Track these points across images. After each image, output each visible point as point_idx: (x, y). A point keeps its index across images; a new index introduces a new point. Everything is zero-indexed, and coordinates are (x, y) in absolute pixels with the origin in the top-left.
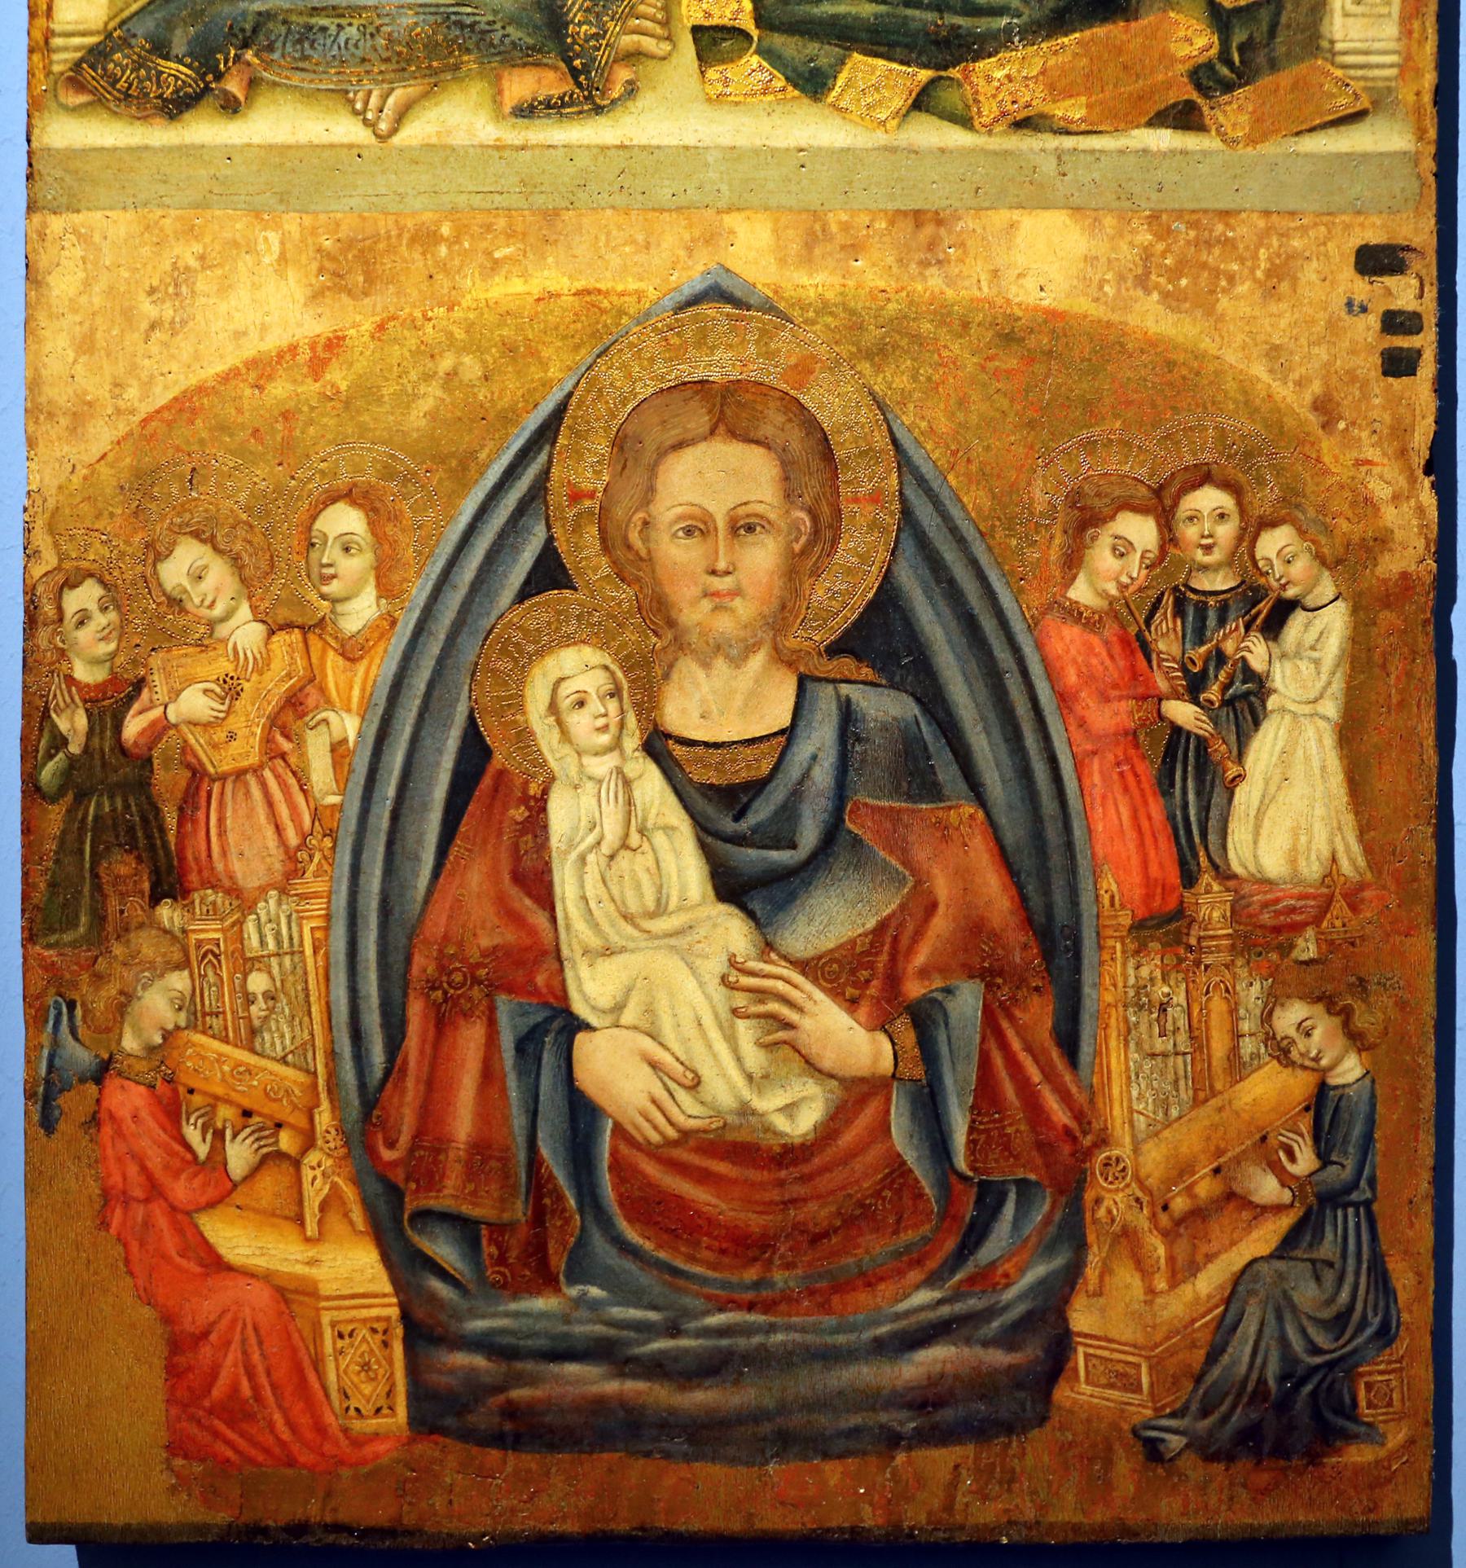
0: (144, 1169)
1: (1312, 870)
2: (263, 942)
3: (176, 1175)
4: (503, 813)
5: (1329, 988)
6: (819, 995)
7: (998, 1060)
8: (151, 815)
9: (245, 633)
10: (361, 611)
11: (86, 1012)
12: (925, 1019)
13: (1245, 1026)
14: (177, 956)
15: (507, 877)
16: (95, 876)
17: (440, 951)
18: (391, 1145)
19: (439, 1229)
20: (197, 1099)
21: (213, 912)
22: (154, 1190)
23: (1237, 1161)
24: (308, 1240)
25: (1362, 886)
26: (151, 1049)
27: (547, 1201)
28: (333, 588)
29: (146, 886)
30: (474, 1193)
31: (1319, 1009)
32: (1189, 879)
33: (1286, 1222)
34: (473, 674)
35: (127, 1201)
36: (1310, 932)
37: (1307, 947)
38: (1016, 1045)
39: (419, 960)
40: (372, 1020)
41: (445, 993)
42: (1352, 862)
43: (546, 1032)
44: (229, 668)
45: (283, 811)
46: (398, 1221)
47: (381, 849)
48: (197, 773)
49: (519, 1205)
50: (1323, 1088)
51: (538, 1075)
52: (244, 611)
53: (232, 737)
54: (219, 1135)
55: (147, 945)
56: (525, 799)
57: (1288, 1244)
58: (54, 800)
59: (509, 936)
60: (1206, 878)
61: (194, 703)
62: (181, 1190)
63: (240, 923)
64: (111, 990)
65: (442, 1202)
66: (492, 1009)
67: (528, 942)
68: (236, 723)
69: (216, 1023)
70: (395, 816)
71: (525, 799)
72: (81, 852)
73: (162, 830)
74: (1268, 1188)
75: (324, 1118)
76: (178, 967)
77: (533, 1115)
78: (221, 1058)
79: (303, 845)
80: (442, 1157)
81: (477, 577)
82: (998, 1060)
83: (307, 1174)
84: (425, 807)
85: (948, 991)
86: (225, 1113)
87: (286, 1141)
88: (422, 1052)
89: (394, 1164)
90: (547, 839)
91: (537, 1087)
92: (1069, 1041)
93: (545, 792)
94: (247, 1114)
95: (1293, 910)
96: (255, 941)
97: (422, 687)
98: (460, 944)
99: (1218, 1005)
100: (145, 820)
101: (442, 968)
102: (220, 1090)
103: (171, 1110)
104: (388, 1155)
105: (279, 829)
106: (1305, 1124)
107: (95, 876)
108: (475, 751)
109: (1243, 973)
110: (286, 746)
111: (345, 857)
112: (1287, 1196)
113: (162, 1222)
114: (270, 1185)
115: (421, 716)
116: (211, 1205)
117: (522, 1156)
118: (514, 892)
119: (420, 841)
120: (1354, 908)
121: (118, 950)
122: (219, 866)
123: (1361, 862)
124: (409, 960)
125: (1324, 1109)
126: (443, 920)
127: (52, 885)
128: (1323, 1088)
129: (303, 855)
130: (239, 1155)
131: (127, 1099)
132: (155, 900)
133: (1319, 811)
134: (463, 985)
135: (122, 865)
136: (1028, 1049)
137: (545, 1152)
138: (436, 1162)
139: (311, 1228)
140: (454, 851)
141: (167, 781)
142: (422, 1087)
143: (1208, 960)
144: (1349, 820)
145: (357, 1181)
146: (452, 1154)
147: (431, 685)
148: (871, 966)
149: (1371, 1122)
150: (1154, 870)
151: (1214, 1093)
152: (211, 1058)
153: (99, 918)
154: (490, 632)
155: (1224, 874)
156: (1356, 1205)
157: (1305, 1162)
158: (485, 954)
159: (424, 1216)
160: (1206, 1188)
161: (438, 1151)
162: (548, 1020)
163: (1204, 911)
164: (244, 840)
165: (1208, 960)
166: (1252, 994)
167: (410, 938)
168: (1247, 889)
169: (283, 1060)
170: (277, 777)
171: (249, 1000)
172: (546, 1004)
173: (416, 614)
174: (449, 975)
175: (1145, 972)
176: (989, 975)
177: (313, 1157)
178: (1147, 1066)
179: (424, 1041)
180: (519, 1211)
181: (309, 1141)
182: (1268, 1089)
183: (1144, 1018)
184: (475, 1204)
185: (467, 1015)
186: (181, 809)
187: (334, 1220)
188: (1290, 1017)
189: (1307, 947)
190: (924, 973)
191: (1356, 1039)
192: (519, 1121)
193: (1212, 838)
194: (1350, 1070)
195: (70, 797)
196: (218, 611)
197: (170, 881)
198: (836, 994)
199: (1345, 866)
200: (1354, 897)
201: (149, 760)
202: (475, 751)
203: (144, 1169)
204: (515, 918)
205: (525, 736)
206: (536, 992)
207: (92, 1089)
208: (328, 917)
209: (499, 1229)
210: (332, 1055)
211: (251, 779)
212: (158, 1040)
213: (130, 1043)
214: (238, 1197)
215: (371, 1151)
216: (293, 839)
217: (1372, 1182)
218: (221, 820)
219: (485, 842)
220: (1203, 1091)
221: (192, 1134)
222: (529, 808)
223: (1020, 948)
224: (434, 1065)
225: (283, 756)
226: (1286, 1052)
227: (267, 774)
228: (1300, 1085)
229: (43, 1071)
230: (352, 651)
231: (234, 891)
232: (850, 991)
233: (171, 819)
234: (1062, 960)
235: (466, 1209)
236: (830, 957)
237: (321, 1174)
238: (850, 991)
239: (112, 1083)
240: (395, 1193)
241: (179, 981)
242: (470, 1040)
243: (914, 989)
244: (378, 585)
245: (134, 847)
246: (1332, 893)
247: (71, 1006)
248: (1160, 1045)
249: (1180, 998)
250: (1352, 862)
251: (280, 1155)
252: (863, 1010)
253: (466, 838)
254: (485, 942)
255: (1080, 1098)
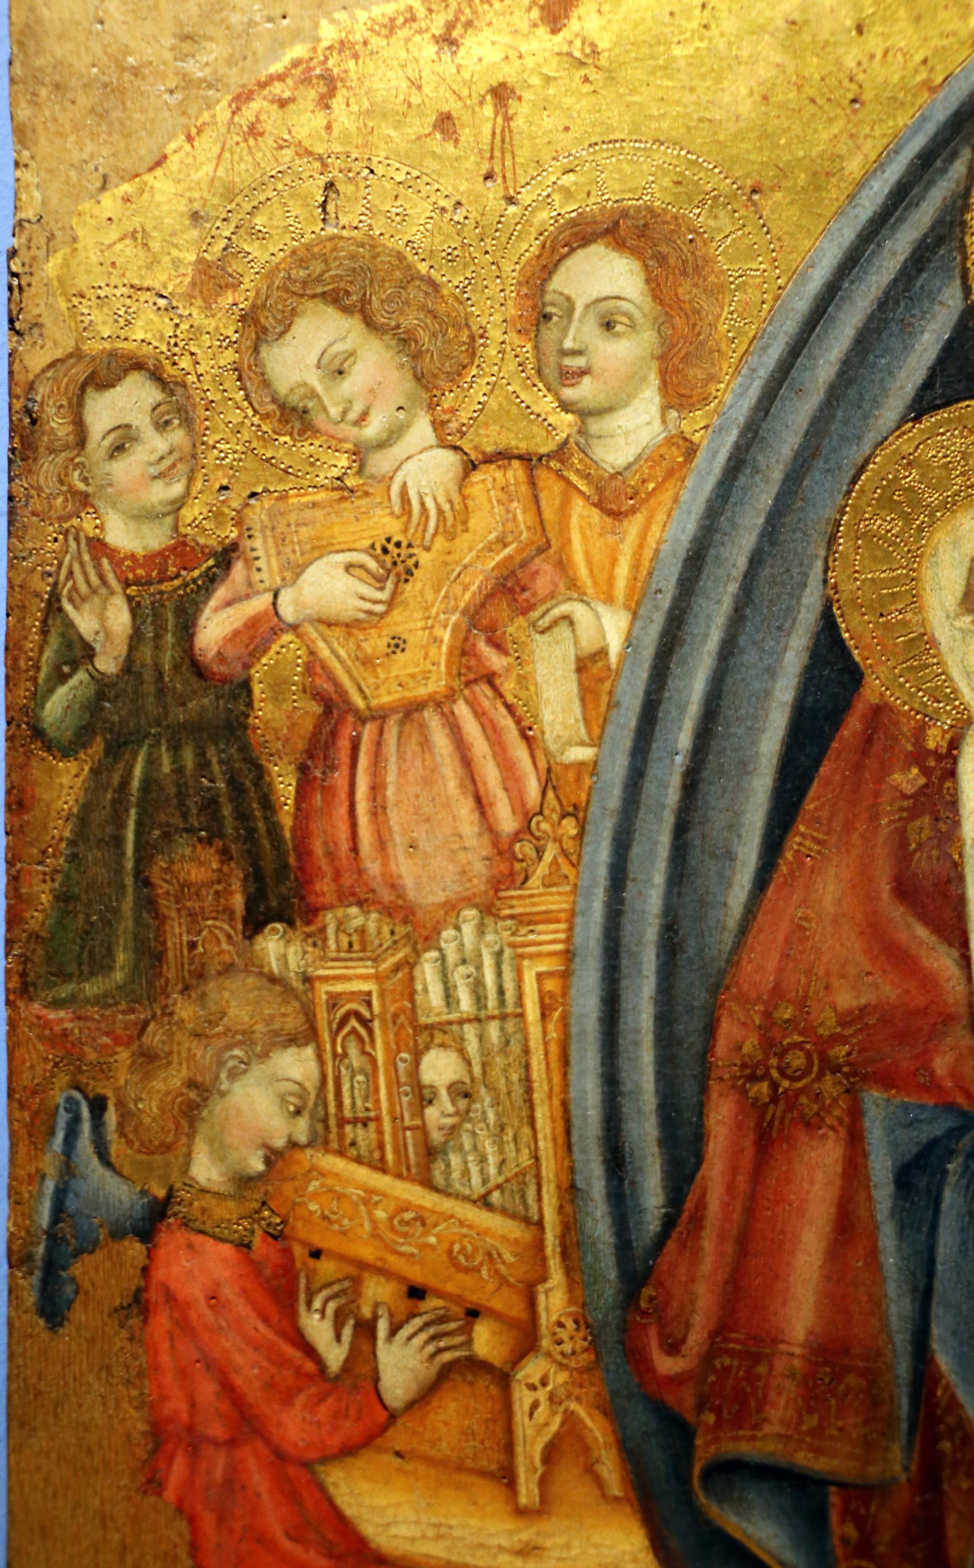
0: (228, 1388)
2: (449, 997)
3: (287, 1399)
4: (880, 780)
8: (249, 781)
9: (424, 468)
10: (634, 430)
11: (125, 1115)
14: (293, 1022)
15: (885, 888)
16: (143, 881)
17: (767, 1015)
18: (673, 1348)
19: (753, 1493)
20: (327, 1268)
21: (360, 946)
22: (246, 1423)
24: (521, 1512)
26: (244, 1182)
27: (946, 1446)
28: (583, 392)
29: (238, 901)
30: (818, 1432)
34: (832, 540)
35: (195, 1443)
39: (728, 1029)
40: (644, 1131)
41: (774, 1086)
43: (950, 1154)
44: (393, 527)
45: (491, 774)
46: (685, 1481)
47: (665, 839)
48: (333, 708)
49: (896, 1452)
51: (934, 1227)
52: (422, 431)
53: (397, 645)
54: (366, 1329)
55: (237, 1002)
56: (919, 756)
58: (67, 751)
59: (887, 990)
61: (329, 586)
62: (295, 1425)
63: (409, 965)
64: (171, 1080)
65: (764, 1444)
66: (856, 1113)
67: (920, 1000)
68: (405, 621)
69: (364, 1137)
70: (692, 783)
71: (919, 756)
72: (118, 841)
73: (268, 805)
75: (554, 1301)
76: (293, 1040)
77: (924, 1297)
78: (370, 1197)
79: (525, 830)
80: (762, 1369)
81: (841, 374)
83: (522, 1398)
84: (745, 768)
86: (377, 1291)
87: (486, 1341)
88: (730, 1188)
89: (676, 1381)
90: (957, 824)
91: (932, 1248)
93: (955, 744)
94: (416, 1293)
96: (435, 997)
97: (742, 562)
98: (802, 1004)
100: (234, 784)
101: (768, 1044)
102: (368, 1253)
103: (280, 1287)
104: (666, 1365)
105: (481, 804)
107: (143, 881)
108: (834, 669)
110: (495, 661)
111: (600, 853)
113: (259, 1480)
114: (453, 1416)
115: (738, 618)
116: (348, 1451)
117: (903, 1368)
118: (897, 914)
119: (734, 827)
121: (185, 1010)
122: (373, 867)
124: (710, 1030)
126: (772, 964)
127: (64, 898)
129: (525, 849)
130: (401, 1364)
131: (198, 1267)
132: (255, 923)
134: (807, 1072)
135: (195, 864)
137: (944, 1361)
138: (751, 1377)
139: (527, 1492)
140: (794, 842)
141: (276, 713)
142: (729, 1248)
145: (611, 1410)
146: (780, 1364)
147: (756, 560)
152: (354, 1196)
153: (151, 956)
154: (862, 469)
158: (845, 1019)
159: (728, 1472)
161: (757, 1358)
162: (955, 1134)
164: (419, 822)
167: (715, 990)
169: (484, 1202)
170: (480, 714)
171: (424, 1097)
172: (950, 1107)
173: (732, 437)
174: (781, 1056)
177: (532, 1369)
179: (734, 1170)
180: (896, 1462)
181: (527, 1339)
184: (818, 1451)
185: (810, 1126)
186: (303, 769)
187: (569, 1478)
192: (899, 1307)
195: (98, 747)
196: (373, 429)
197: (280, 891)
201: (246, 685)
202: (834, 669)
203: (228, 1388)
204: (896, 957)
205: (923, 644)
206: (933, 1086)
207: (135, 1249)
208: (569, 955)
209: (860, 1494)
210: (571, 1192)
211: (432, 718)
212: (257, 1165)
213: (205, 1170)
214: (398, 1437)
215: (637, 1359)
216: (507, 821)
218: (376, 789)
219: (848, 827)
221: (317, 1327)
222: (925, 771)
224: (750, 1212)
225: (490, 679)
227: (462, 709)
229: (44, 1215)
230: (615, 500)
231: (399, 910)
233: (285, 785)
235: (803, 1459)
237: (545, 1399)
239: (172, 1240)
240: (679, 1432)
241: (297, 1065)
242: (816, 1168)
244: (664, 387)
245: (215, 833)
247: (98, 1106)
251: (475, 1365)
253: (815, 821)
254: (846, 999)
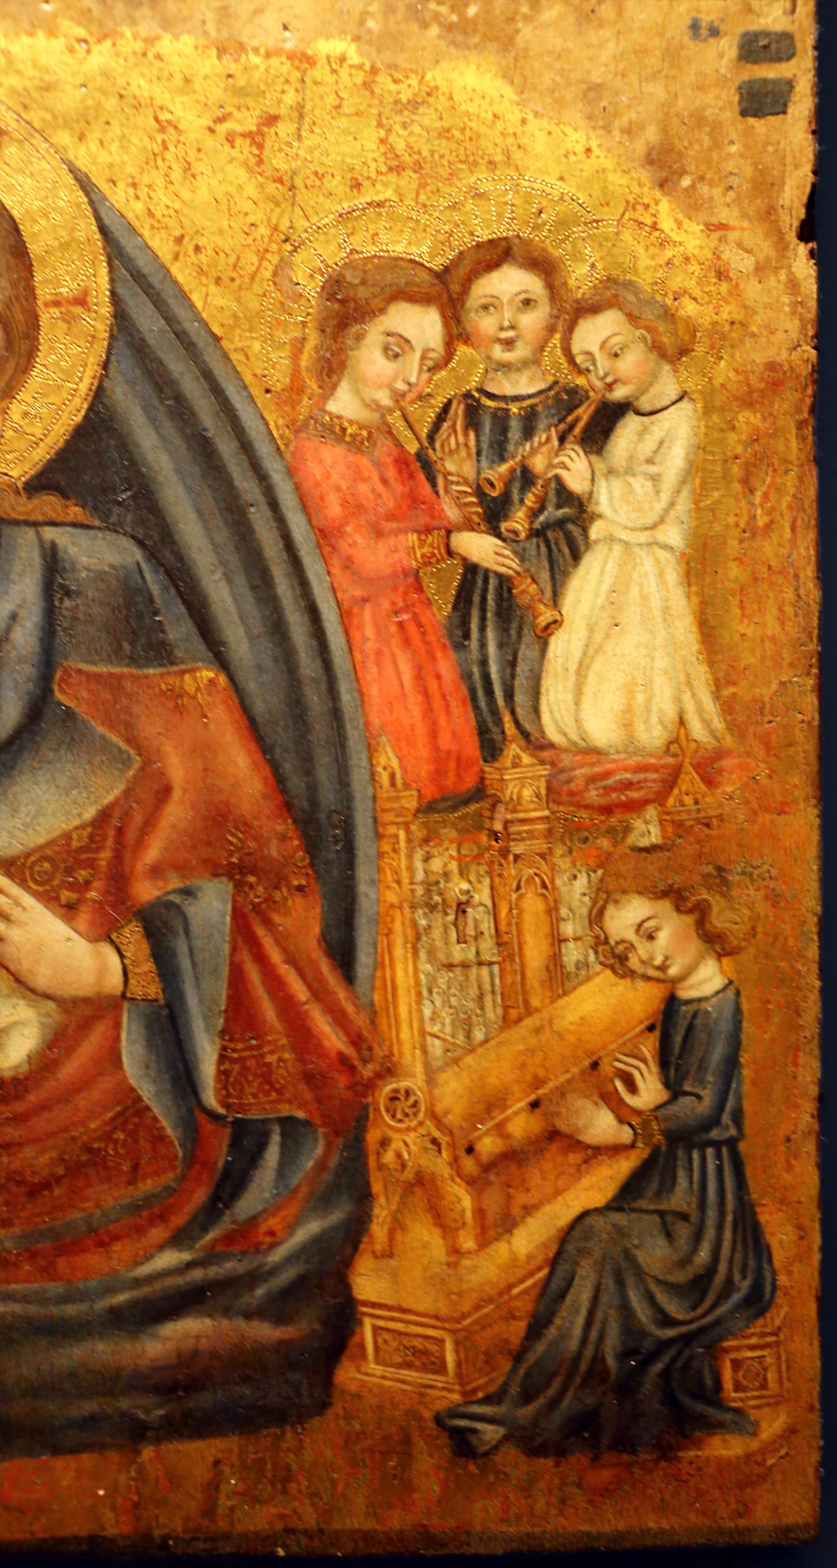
1: (652, 736)
5: (677, 880)
6: (28, 900)
7: (253, 974)
12: (160, 928)
13: (568, 929)
23: (561, 1092)
25: (719, 754)
31: (665, 906)
32: (491, 749)
33: (625, 1166)
36: (651, 812)
37: (647, 830)
38: (276, 956)
42: (705, 724)
50: (672, 1004)
57: (629, 1193)
60: (513, 749)
74: (601, 1125)
82: (253, 974)
85: (188, 892)
92: (342, 952)
95: (628, 785)
99: (533, 904)
106: (649, 1047)
109: (564, 864)
112: (626, 1135)
120: (709, 782)
123: (718, 724)
125: (675, 1030)
128: (672, 1004)
133: (661, 663)
136: (291, 961)
143: (518, 848)
144: (701, 673)
148: (91, 864)
149: (735, 1044)
150: (445, 742)
151: (529, 1011)
155: (536, 743)
156: (717, 1145)
157: (650, 1091)
160: (521, 1125)
163: (511, 790)
165: (518, 848)
166: (576, 890)
168: (566, 760)
175: (436, 865)
176: (239, 872)
178: (443, 979)
182: (600, 1005)
183: (438, 920)
188: (626, 917)
189: (647, 830)
190: (156, 872)
191: (715, 942)
193: (520, 698)
194: (706, 980)
198: (49, 898)
199: (697, 730)
200: (709, 769)
217: (738, 1117)
220: (515, 1008)
223: (279, 841)
226: (623, 959)
228: (642, 1000)
232: (66, 895)
234: (332, 851)
236: (41, 853)
238: (66, 895)
243: (146, 891)
246: (680, 765)
248: (458, 953)
249: (483, 895)
250: (705, 724)
252: (84, 917)
255: (360, 1020)
